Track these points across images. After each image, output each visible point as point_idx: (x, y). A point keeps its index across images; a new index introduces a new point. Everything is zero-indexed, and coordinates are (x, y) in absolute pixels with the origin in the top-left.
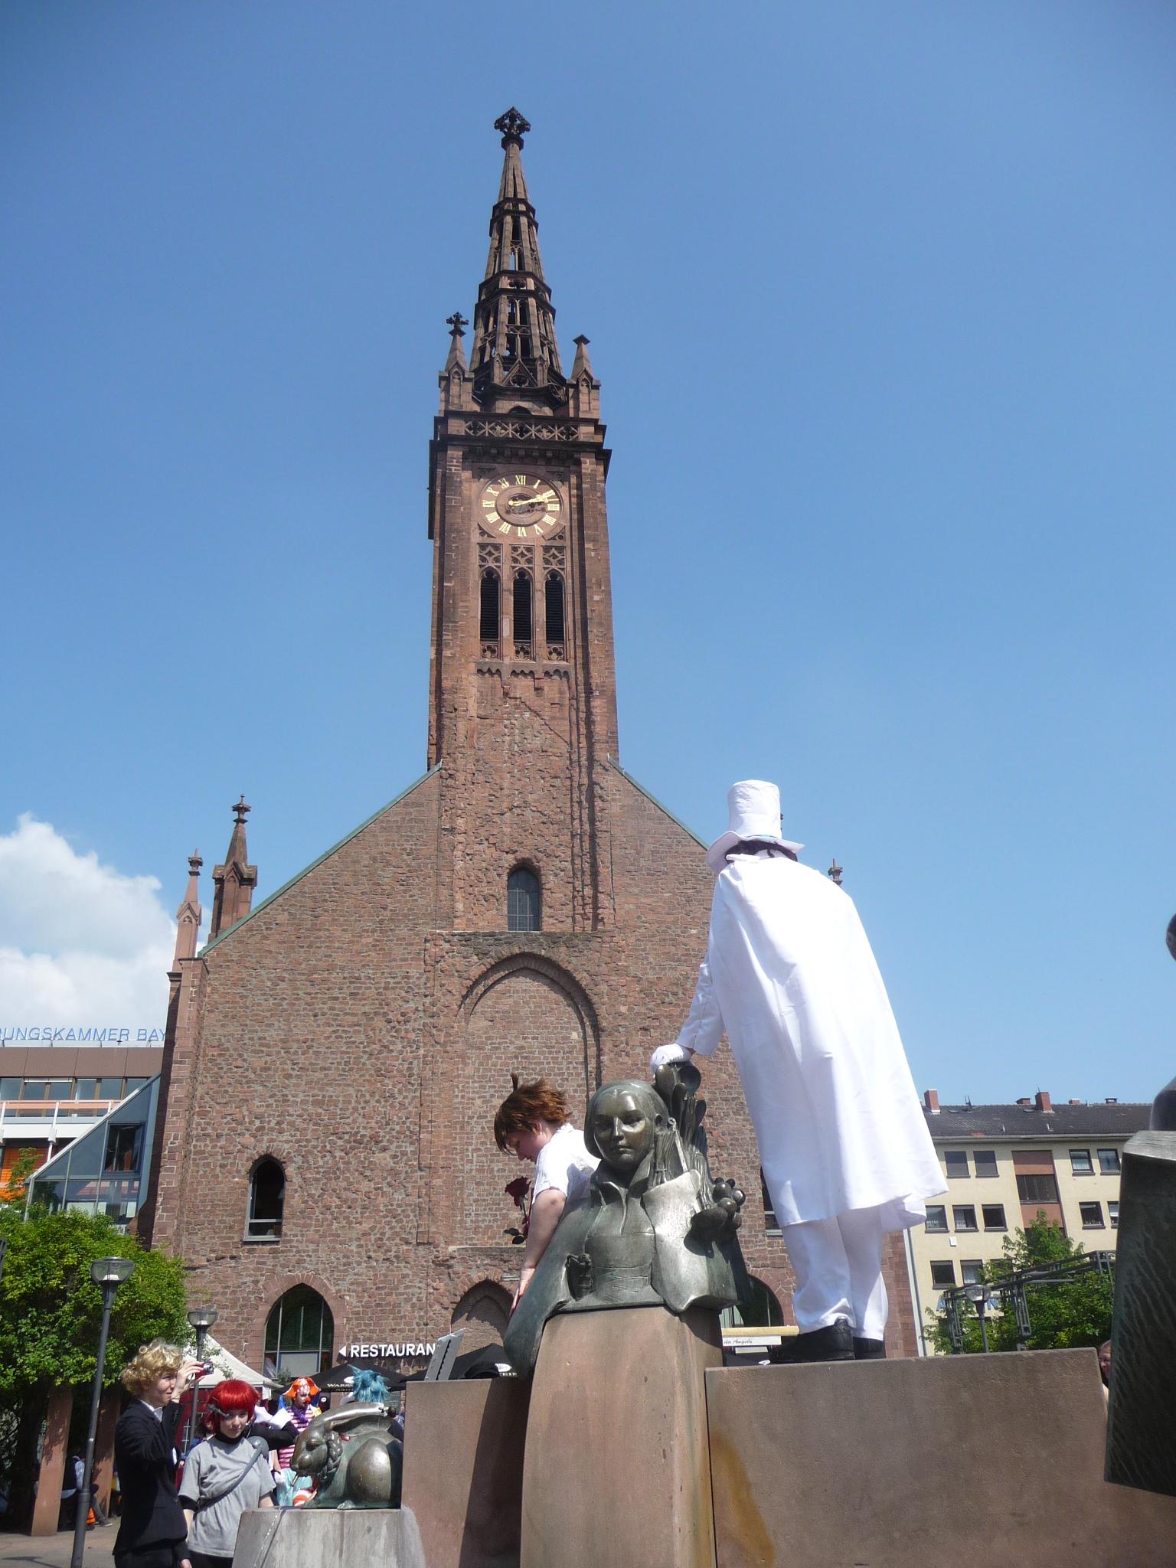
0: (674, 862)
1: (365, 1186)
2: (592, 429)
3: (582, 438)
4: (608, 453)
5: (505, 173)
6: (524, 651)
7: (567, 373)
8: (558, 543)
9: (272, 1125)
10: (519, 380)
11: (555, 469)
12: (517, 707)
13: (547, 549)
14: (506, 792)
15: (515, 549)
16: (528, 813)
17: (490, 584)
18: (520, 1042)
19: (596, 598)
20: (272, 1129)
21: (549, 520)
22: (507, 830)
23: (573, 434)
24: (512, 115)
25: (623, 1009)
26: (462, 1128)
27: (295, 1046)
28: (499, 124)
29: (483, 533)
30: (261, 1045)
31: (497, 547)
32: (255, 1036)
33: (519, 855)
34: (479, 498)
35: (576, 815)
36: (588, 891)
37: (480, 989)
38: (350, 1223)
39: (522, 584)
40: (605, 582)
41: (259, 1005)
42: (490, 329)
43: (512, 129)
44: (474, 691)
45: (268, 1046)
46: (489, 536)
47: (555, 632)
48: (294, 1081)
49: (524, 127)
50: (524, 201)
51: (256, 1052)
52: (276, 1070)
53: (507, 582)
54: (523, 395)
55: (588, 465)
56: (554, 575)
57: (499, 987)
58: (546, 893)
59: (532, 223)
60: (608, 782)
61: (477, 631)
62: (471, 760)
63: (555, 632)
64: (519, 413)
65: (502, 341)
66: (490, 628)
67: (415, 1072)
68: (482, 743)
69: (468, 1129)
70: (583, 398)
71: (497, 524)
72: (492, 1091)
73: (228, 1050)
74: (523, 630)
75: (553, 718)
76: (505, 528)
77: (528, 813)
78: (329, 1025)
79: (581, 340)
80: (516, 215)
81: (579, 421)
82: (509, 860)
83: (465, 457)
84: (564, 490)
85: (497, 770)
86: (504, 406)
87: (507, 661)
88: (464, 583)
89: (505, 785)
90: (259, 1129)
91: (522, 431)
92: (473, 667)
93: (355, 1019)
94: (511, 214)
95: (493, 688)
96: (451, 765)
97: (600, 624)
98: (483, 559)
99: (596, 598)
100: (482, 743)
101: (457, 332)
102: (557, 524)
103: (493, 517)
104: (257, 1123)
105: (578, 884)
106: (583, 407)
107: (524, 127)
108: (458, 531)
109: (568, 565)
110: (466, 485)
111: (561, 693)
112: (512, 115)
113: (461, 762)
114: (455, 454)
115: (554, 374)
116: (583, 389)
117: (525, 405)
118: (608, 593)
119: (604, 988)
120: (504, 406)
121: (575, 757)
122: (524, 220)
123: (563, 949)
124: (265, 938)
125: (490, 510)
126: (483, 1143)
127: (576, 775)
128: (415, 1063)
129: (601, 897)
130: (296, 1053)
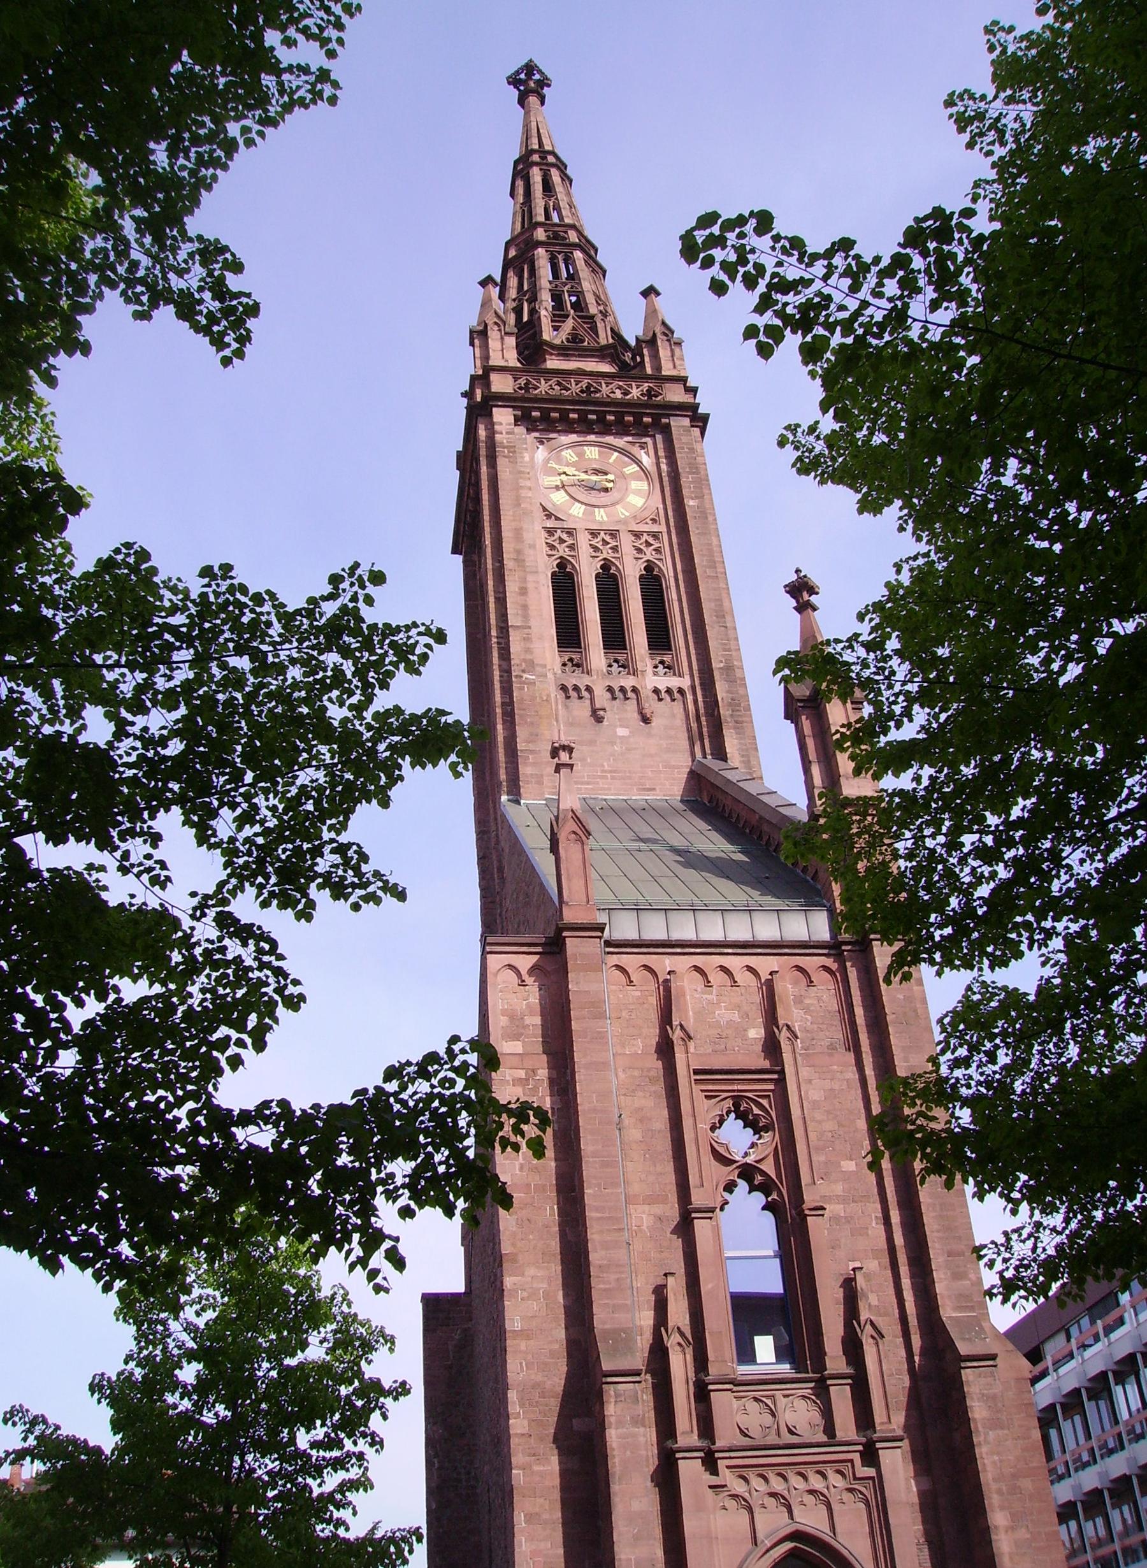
4: (705, 419)
7: (632, 332)
15: (594, 534)
29: (549, 516)
31: (570, 532)
43: (529, 84)
46: (557, 519)
50: (553, 153)
55: (680, 424)
63: (659, 639)
66: (569, 634)
74: (615, 636)
76: (578, 510)
79: (650, 292)
83: (517, 421)
94: (536, 168)
114: (503, 417)
115: (616, 334)
116: (661, 342)
122: (555, 175)
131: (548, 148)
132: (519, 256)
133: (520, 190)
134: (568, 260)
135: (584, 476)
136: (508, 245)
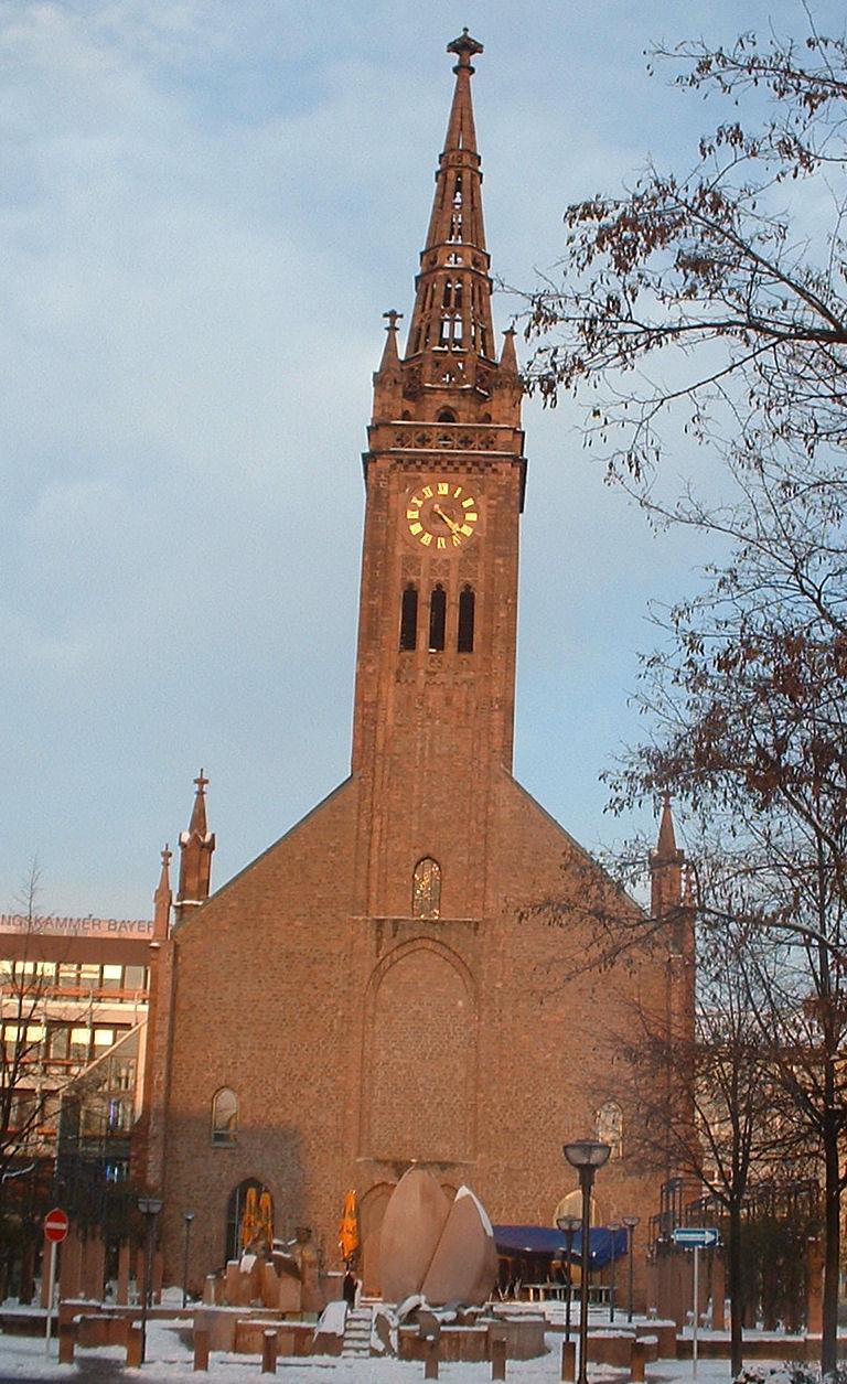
1: (297, 1111)
2: (510, 435)
9: (229, 1064)
11: (475, 477)
12: (429, 716)
15: (435, 561)
17: (410, 597)
18: (416, 1008)
19: (502, 615)
25: (499, 985)
26: (370, 1072)
31: (418, 560)
32: (216, 996)
38: (285, 1137)
39: (439, 597)
41: (218, 972)
44: (391, 701)
47: (465, 644)
48: (244, 1031)
53: (425, 596)
61: (397, 644)
63: (465, 644)
66: (409, 641)
67: (335, 1027)
69: (374, 1073)
71: (421, 535)
72: (394, 1045)
74: (437, 640)
76: (427, 539)
93: (289, 987)
97: (503, 640)
99: (502, 615)
101: (392, 329)
103: (416, 529)
104: (218, 1062)
108: (385, 549)
111: (468, 702)
119: (484, 967)
125: (414, 521)
126: (386, 1083)
128: (335, 1021)
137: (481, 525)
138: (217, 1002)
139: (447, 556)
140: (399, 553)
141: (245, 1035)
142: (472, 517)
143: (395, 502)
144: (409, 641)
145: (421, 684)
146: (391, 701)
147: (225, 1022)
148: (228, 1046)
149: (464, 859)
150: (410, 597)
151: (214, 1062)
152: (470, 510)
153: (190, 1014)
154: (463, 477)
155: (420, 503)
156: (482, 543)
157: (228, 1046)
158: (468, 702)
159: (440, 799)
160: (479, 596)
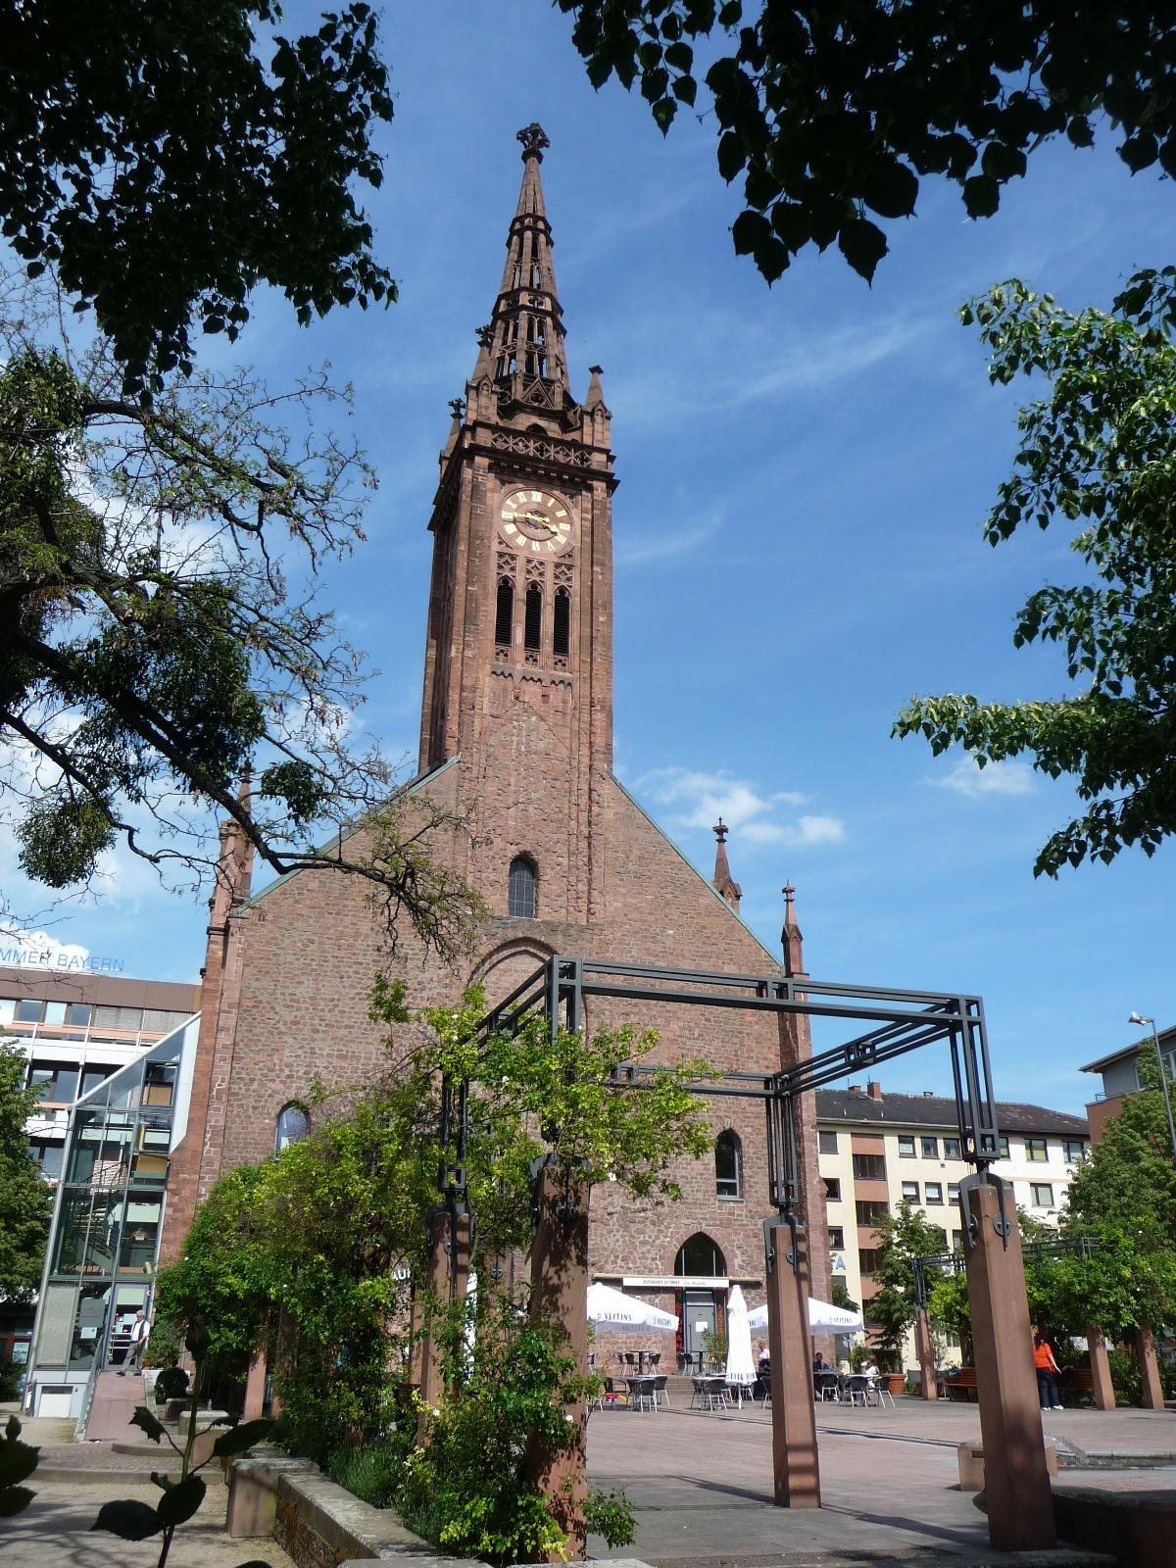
0: (656, 868)
2: (604, 457)
3: (595, 466)
5: (525, 186)
6: (531, 658)
7: (581, 398)
8: (567, 561)
9: (301, 1074)
10: (537, 398)
13: (557, 566)
14: (513, 788)
16: (531, 808)
17: (505, 591)
19: (601, 619)
20: (299, 1078)
21: (561, 539)
22: (511, 823)
23: (587, 460)
24: (535, 130)
27: (323, 1003)
28: (522, 136)
30: (292, 1000)
31: (513, 557)
33: (522, 848)
34: (500, 508)
35: (574, 816)
36: (582, 887)
37: (487, 965)
40: (607, 606)
41: (291, 963)
42: (509, 343)
43: (533, 143)
44: (487, 691)
45: (298, 1001)
47: (561, 645)
48: (321, 1035)
49: (544, 143)
50: (543, 219)
51: (288, 1007)
52: (305, 1024)
54: (541, 413)
56: (562, 590)
57: (501, 966)
58: (543, 885)
59: (550, 242)
60: (605, 790)
61: (492, 635)
62: (484, 756)
63: (561, 645)
64: (535, 432)
65: (522, 357)
66: (503, 634)
68: (492, 741)
70: (598, 427)
71: (515, 535)
73: (261, 1002)
74: (532, 639)
75: (556, 725)
76: (521, 540)
77: (531, 808)
78: (353, 987)
79: (596, 370)
80: (536, 232)
81: (592, 449)
82: (513, 851)
83: (490, 468)
84: (576, 514)
85: (506, 767)
86: (523, 421)
87: (518, 666)
88: (485, 588)
89: (512, 781)
90: (289, 1077)
91: (541, 450)
92: (488, 668)
94: (529, 230)
95: (505, 690)
96: (469, 759)
97: (604, 644)
98: (500, 567)
99: (601, 619)
100: (492, 741)
102: (568, 543)
105: (573, 879)
106: (598, 436)
107: (544, 143)
109: (576, 583)
110: (489, 494)
111: (565, 702)
112: (535, 130)
113: (476, 756)
115: (566, 396)
116: (598, 419)
117: (542, 423)
118: (610, 616)
120: (523, 421)
121: (575, 763)
122: (542, 238)
123: (560, 937)
124: (297, 902)
127: (576, 780)
129: (595, 893)
130: (323, 1010)
131: (539, 214)
132: (507, 309)
133: (515, 246)
134: (541, 324)
135: (529, 515)
136: (500, 298)
137: (575, 536)
138: (288, 998)
139: (542, 559)
140: (495, 547)
141: (323, 1040)
142: (565, 527)
143: (492, 498)
144: (503, 634)
145: (517, 677)
146: (487, 691)
147: (298, 1023)
148: (300, 1052)
149: (565, 861)
150: (505, 591)
151: (281, 1070)
152: (562, 520)
153: (254, 1011)
154: (557, 493)
155: (514, 506)
156: (577, 554)
157: (300, 1052)
158: (565, 702)
159: (537, 795)
160: (575, 603)
